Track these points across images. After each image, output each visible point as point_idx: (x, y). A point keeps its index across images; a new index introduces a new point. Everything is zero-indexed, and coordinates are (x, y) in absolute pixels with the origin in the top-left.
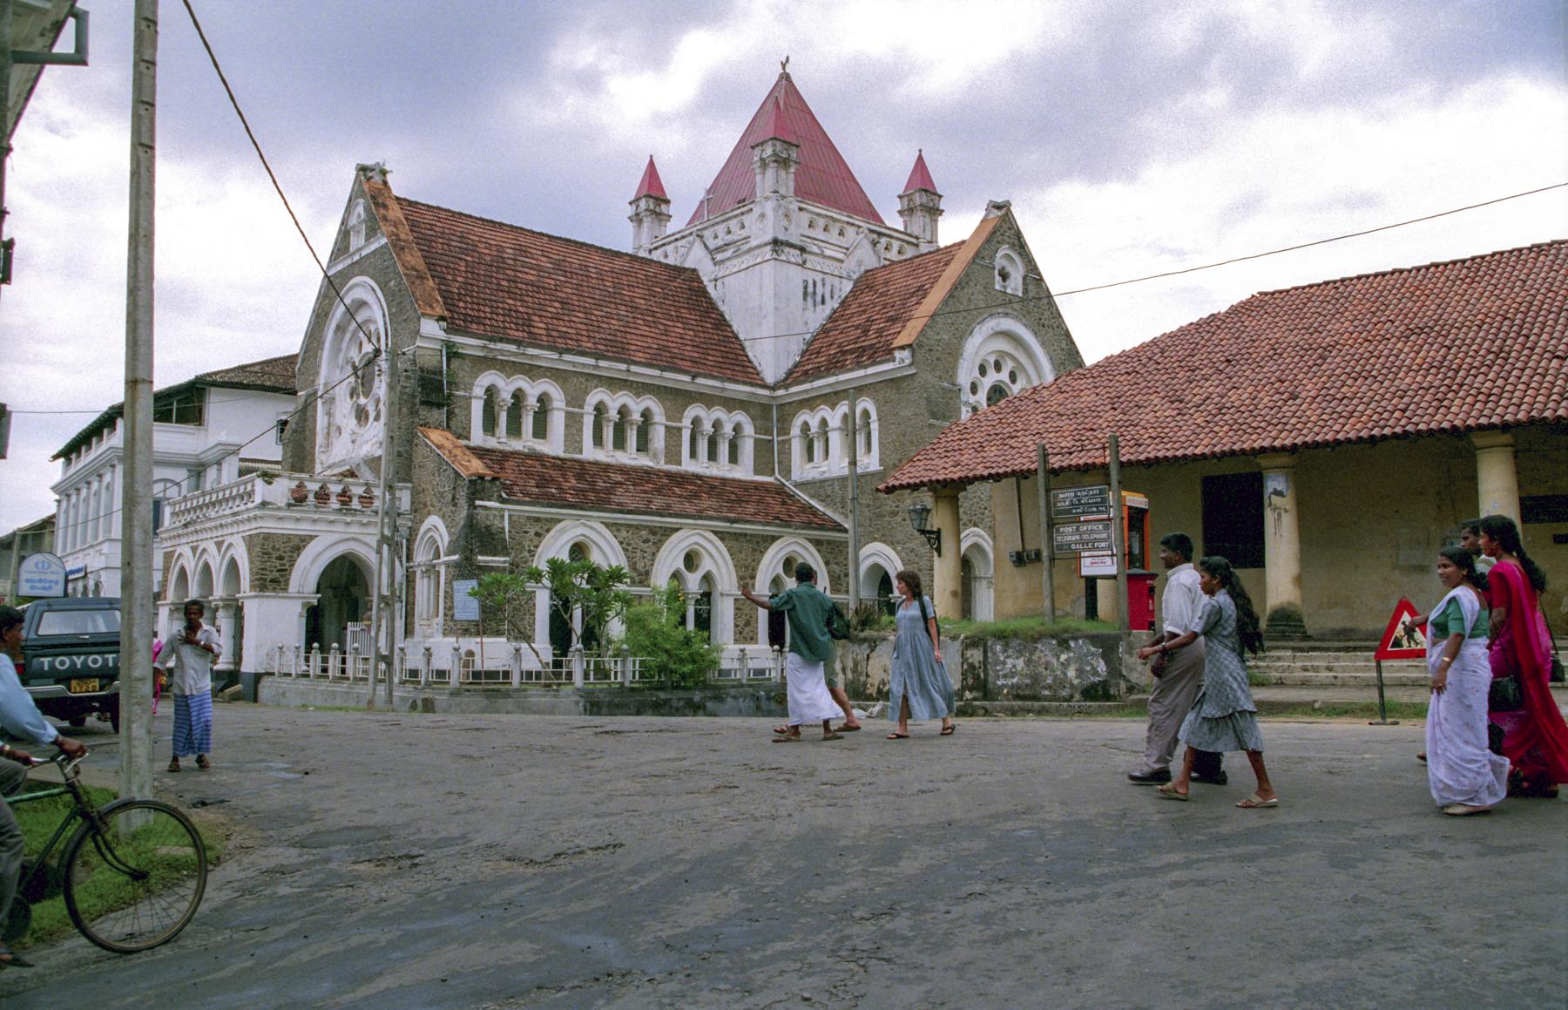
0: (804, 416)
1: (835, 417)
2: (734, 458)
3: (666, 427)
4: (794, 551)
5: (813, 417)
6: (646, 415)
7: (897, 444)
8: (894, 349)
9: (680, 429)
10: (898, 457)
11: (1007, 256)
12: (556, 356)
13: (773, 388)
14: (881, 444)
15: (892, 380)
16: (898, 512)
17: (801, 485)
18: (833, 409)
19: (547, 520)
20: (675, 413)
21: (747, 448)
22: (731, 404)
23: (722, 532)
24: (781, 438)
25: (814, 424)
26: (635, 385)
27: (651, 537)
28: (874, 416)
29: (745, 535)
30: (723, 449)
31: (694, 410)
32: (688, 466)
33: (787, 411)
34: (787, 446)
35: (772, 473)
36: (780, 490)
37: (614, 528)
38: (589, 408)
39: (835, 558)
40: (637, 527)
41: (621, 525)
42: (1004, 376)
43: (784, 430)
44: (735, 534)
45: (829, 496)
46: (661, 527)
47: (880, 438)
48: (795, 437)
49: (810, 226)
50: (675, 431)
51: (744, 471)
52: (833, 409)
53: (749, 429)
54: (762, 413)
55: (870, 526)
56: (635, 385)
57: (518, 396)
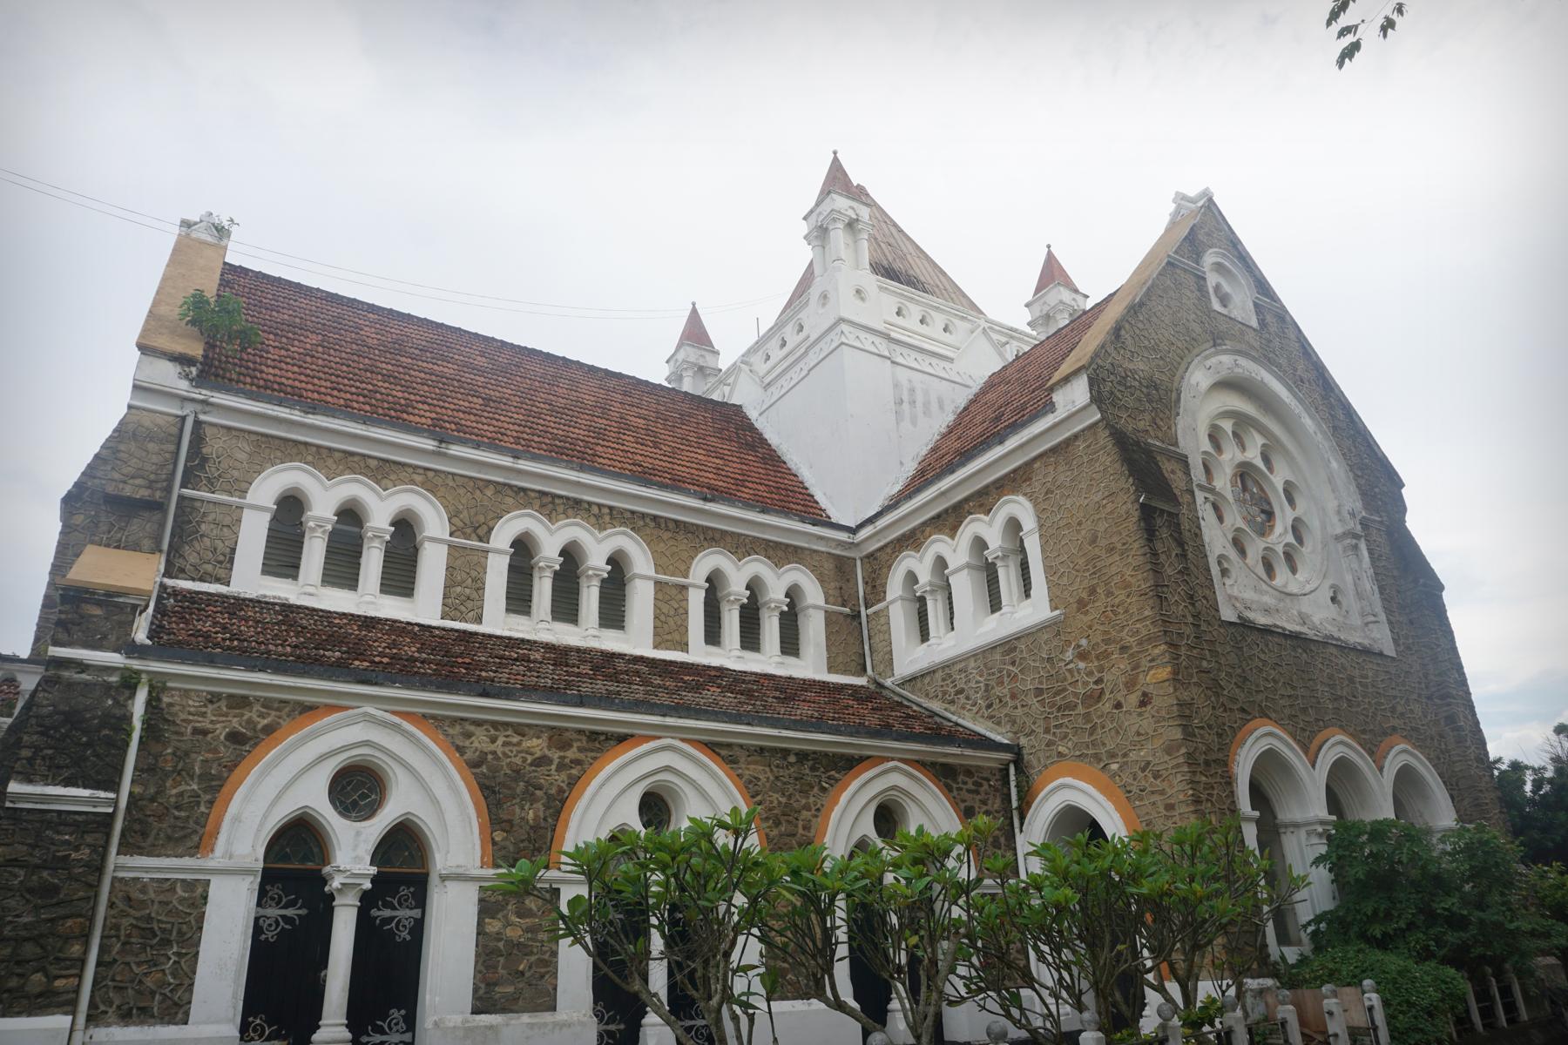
0: (908, 562)
1: (955, 550)
2: (790, 644)
3: (657, 583)
4: (893, 788)
5: (921, 560)
6: (617, 562)
7: (1081, 561)
8: (1052, 389)
9: (684, 588)
10: (1086, 583)
11: (1219, 268)
12: (429, 444)
13: (853, 531)
14: (1049, 571)
15: (1053, 450)
16: (1102, 692)
17: (911, 680)
18: (953, 537)
19: (267, 704)
20: (672, 561)
21: (814, 629)
22: (781, 553)
23: (729, 746)
24: (870, 611)
25: (925, 576)
26: (595, 510)
27: (555, 755)
28: (1029, 522)
29: (785, 753)
30: (771, 629)
31: (706, 562)
32: (699, 653)
33: (879, 563)
34: (882, 620)
35: (862, 670)
36: (873, 696)
37: (457, 729)
38: (503, 535)
39: (984, 802)
40: (520, 730)
41: (478, 723)
42: (1253, 455)
43: (876, 591)
44: (762, 749)
45: (961, 691)
46: (580, 732)
47: (1045, 559)
48: (892, 602)
49: (899, 313)
50: (674, 592)
51: (811, 665)
52: (953, 537)
53: (814, 594)
54: (837, 571)
55: (1047, 731)
56: (595, 510)
57: (351, 515)
